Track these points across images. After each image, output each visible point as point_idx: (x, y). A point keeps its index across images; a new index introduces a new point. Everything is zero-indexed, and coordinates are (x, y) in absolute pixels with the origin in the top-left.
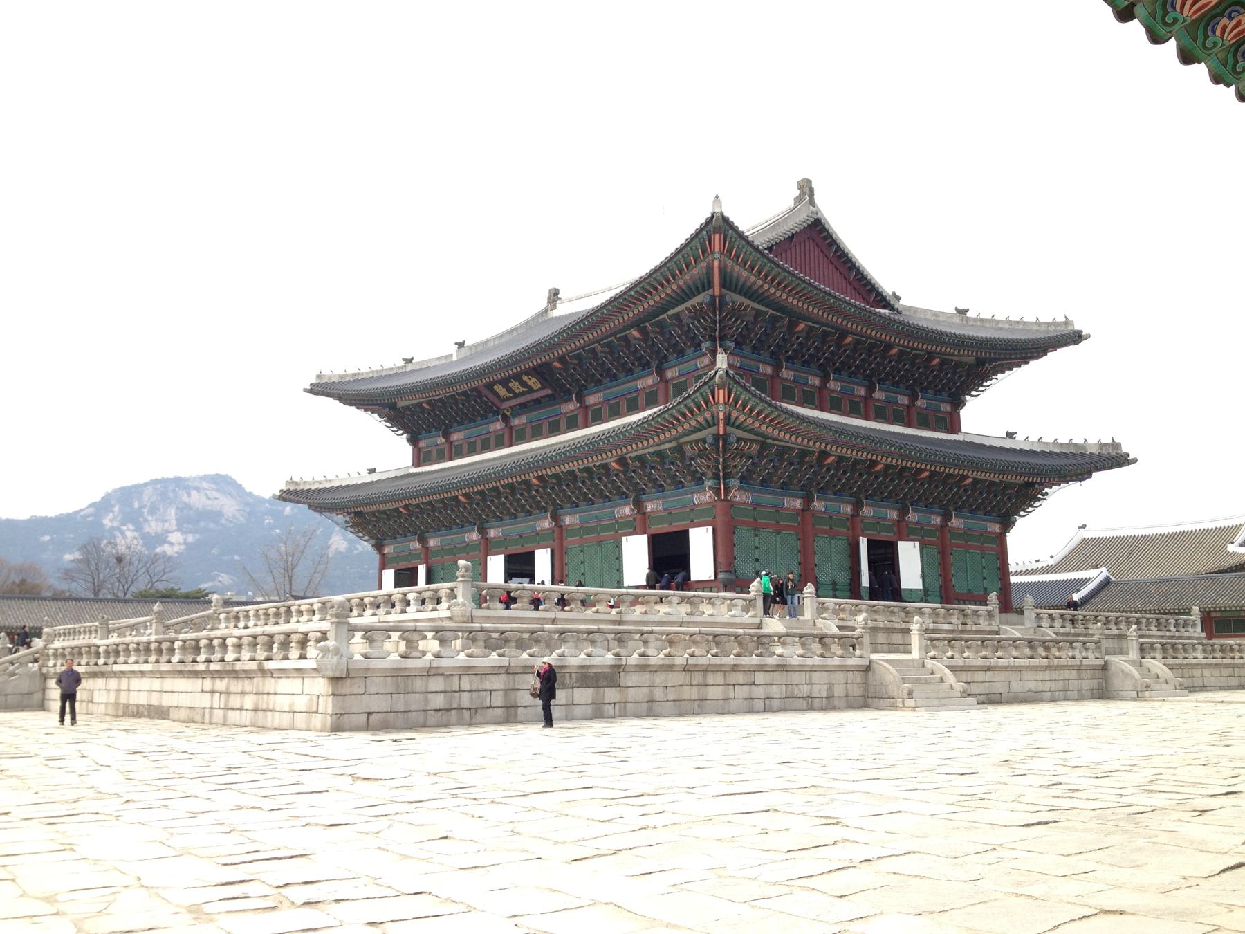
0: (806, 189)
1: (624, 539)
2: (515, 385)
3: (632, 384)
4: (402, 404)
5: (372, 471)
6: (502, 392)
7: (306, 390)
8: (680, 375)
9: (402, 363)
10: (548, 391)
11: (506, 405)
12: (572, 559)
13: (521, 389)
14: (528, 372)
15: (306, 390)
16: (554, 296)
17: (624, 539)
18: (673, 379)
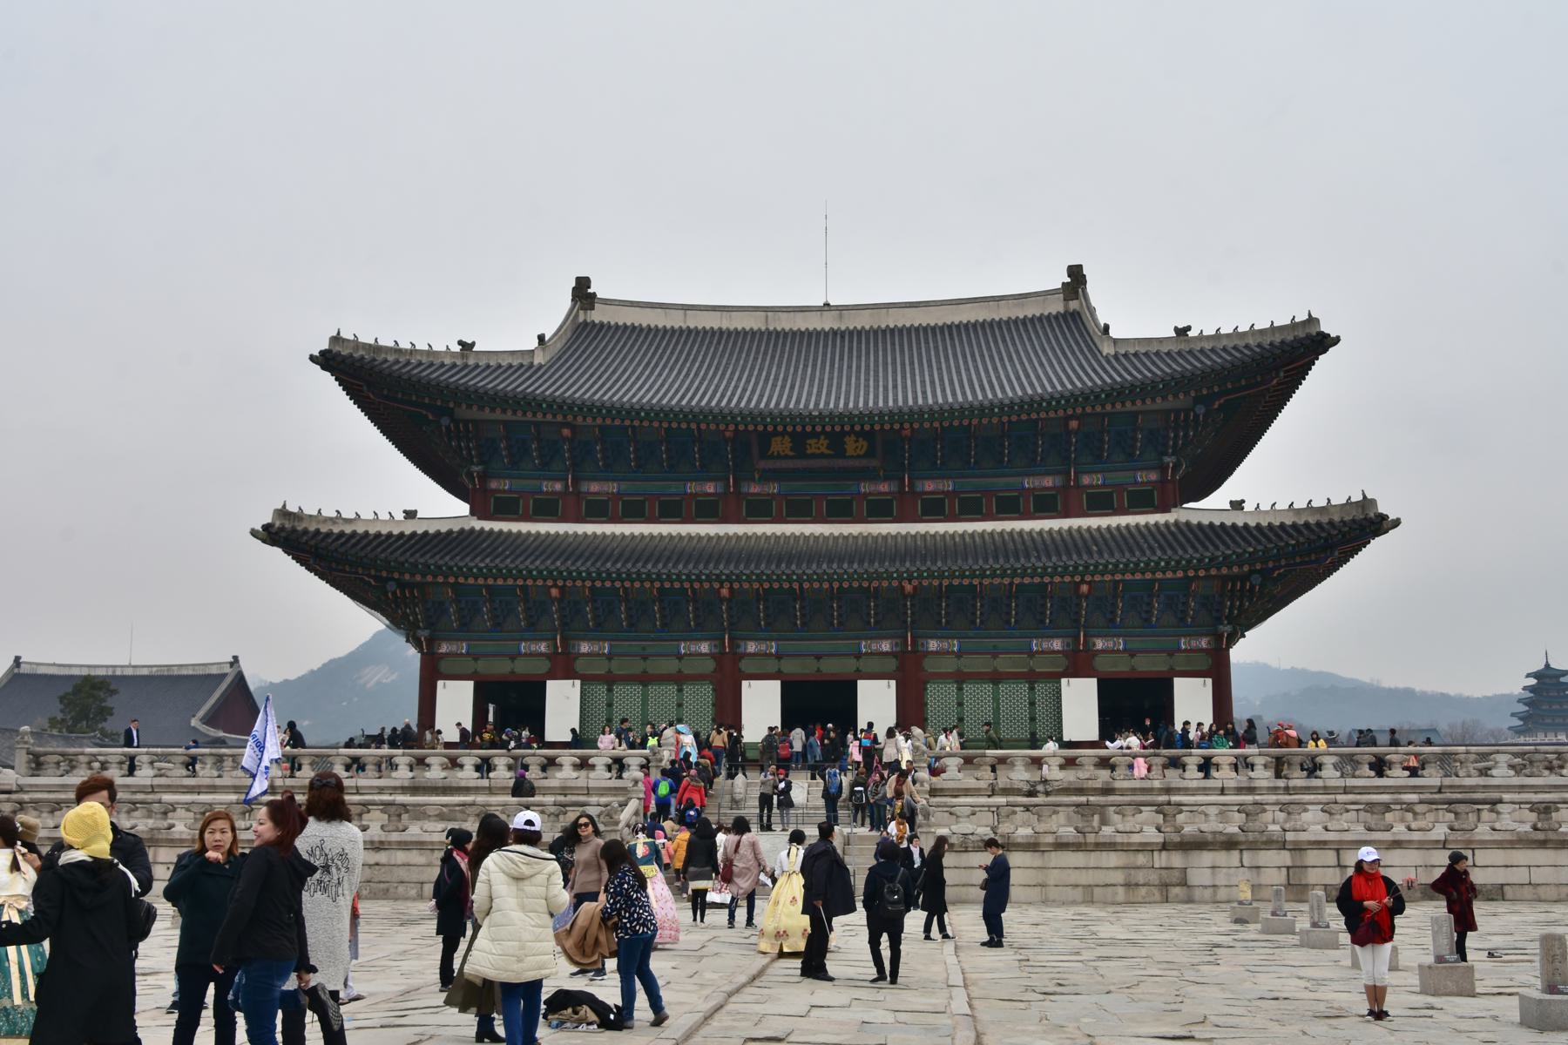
0: (1076, 273)
1: (1064, 681)
2: (819, 446)
3: (1019, 479)
4: (464, 412)
5: (410, 515)
6: (780, 446)
7: (312, 358)
8: (1104, 485)
9: (457, 348)
10: (875, 463)
11: (763, 464)
12: (939, 697)
13: (824, 450)
14: (862, 434)
15: (312, 358)
16: (582, 292)
17: (1064, 681)
18: (1089, 487)
